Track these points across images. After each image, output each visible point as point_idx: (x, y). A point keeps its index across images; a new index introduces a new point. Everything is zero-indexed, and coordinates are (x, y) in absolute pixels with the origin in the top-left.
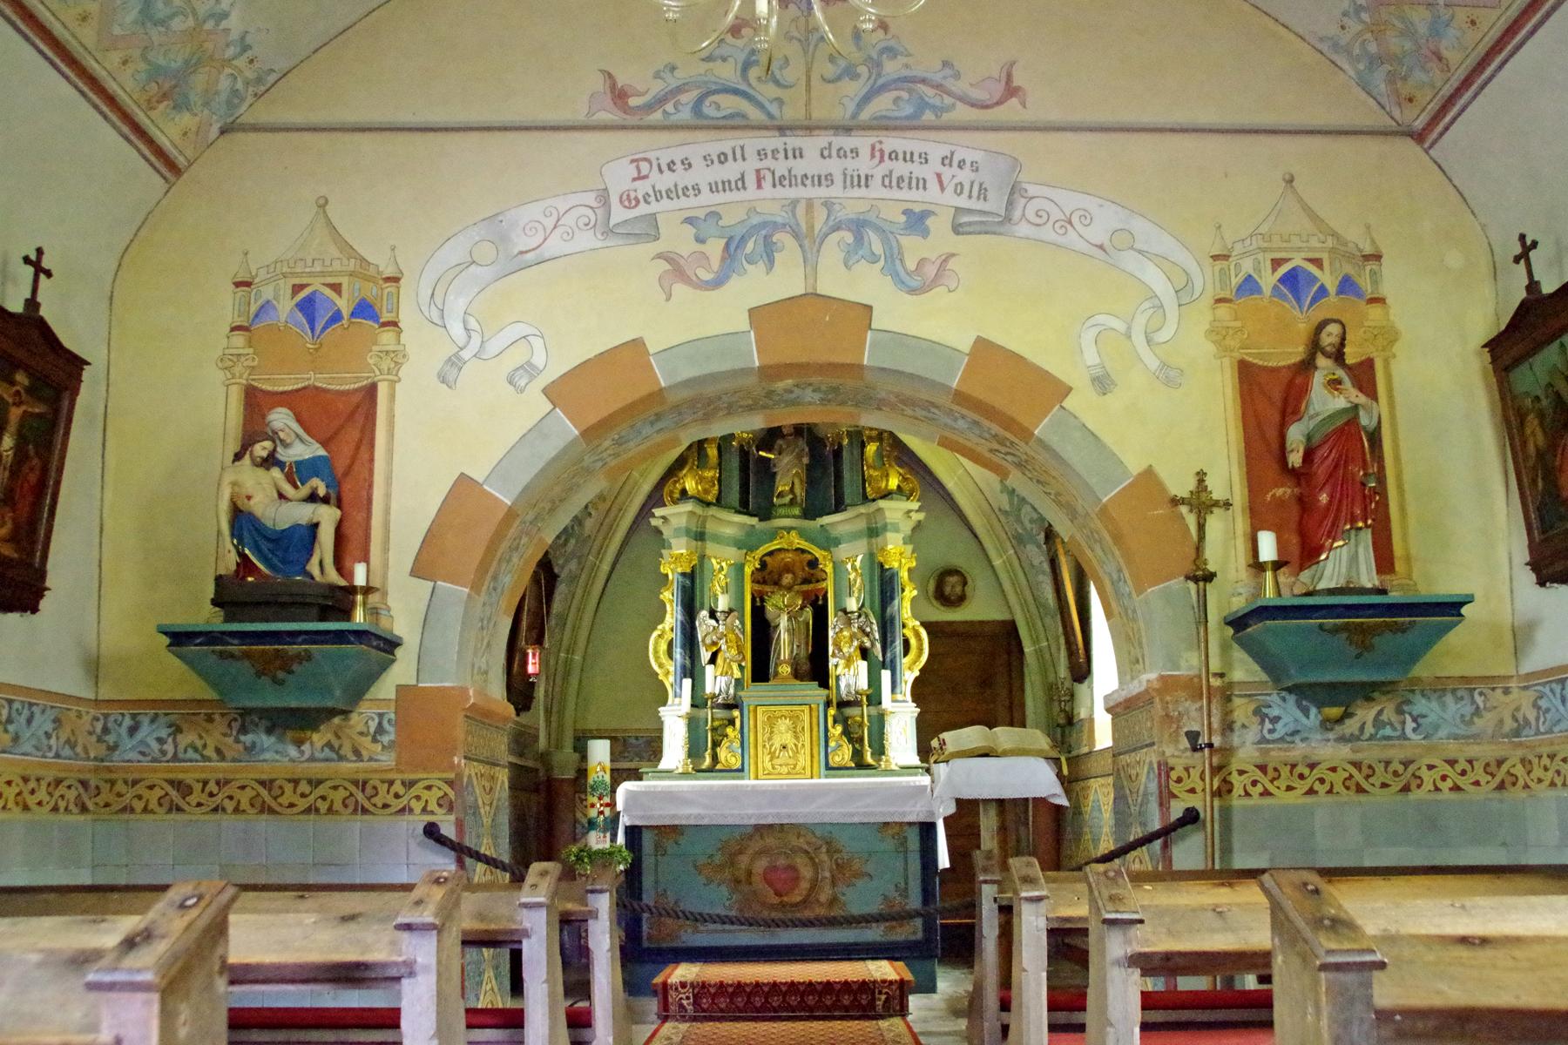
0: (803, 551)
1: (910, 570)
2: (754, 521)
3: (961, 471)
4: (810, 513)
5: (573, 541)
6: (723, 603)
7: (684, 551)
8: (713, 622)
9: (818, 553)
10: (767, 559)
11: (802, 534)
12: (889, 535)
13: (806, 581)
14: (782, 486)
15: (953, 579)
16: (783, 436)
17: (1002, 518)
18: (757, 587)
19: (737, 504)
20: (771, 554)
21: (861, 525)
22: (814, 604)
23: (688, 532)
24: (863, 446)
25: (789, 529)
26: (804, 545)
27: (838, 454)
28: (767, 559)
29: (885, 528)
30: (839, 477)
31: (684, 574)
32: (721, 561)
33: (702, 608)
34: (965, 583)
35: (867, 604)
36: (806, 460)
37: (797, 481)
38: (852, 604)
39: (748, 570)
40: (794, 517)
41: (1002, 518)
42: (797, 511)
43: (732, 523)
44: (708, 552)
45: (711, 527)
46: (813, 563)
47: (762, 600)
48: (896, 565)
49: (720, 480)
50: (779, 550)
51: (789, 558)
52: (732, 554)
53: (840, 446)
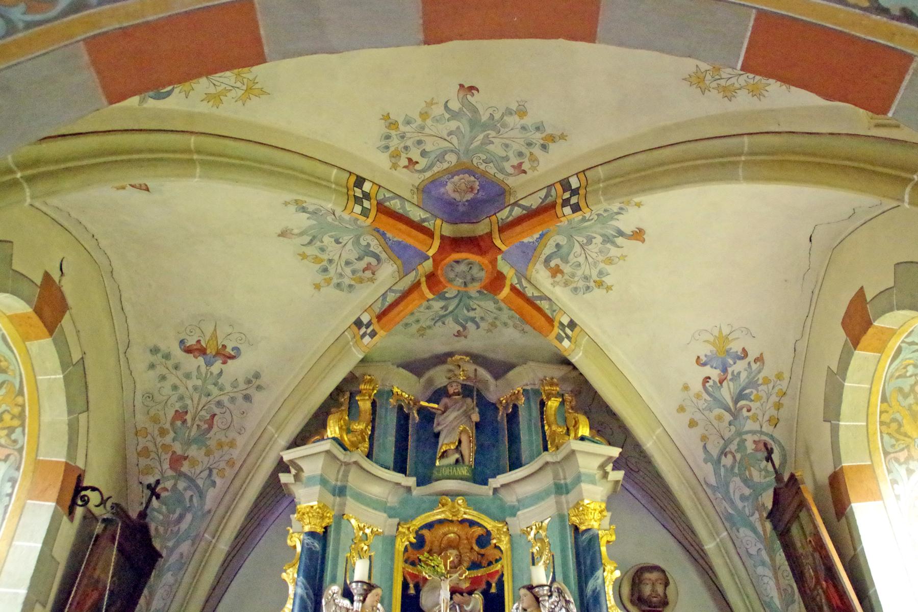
0: (472, 523)
1: (608, 542)
2: (411, 481)
3: (659, 431)
4: (480, 477)
5: (189, 517)
6: (361, 570)
7: (315, 503)
8: (346, 603)
9: (489, 524)
10: (425, 532)
11: (472, 502)
12: (585, 487)
13: (474, 566)
14: (446, 443)
15: (654, 576)
16: (449, 396)
17: (709, 491)
18: (410, 569)
19: (391, 464)
20: (430, 526)
21: (546, 480)
22: (486, 593)
23: (323, 482)
24: (543, 404)
25: (454, 495)
26: (472, 515)
27: (513, 418)
28: (425, 532)
29: (578, 479)
30: (514, 439)
31: (312, 534)
32: (362, 520)
33: (334, 581)
34: (666, 584)
35: (559, 577)
36: (476, 417)
37: (464, 439)
38: (540, 575)
39: (401, 545)
40: (462, 478)
41: (709, 491)
42: (464, 471)
43: (383, 483)
44: (347, 511)
45: (355, 480)
46: (484, 540)
47: (418, 588)
48: (596, 525)
49: (371, 438)
50: (441, 522)
51: (452, 533)
52: (380, 522)
53: (515, 407)
